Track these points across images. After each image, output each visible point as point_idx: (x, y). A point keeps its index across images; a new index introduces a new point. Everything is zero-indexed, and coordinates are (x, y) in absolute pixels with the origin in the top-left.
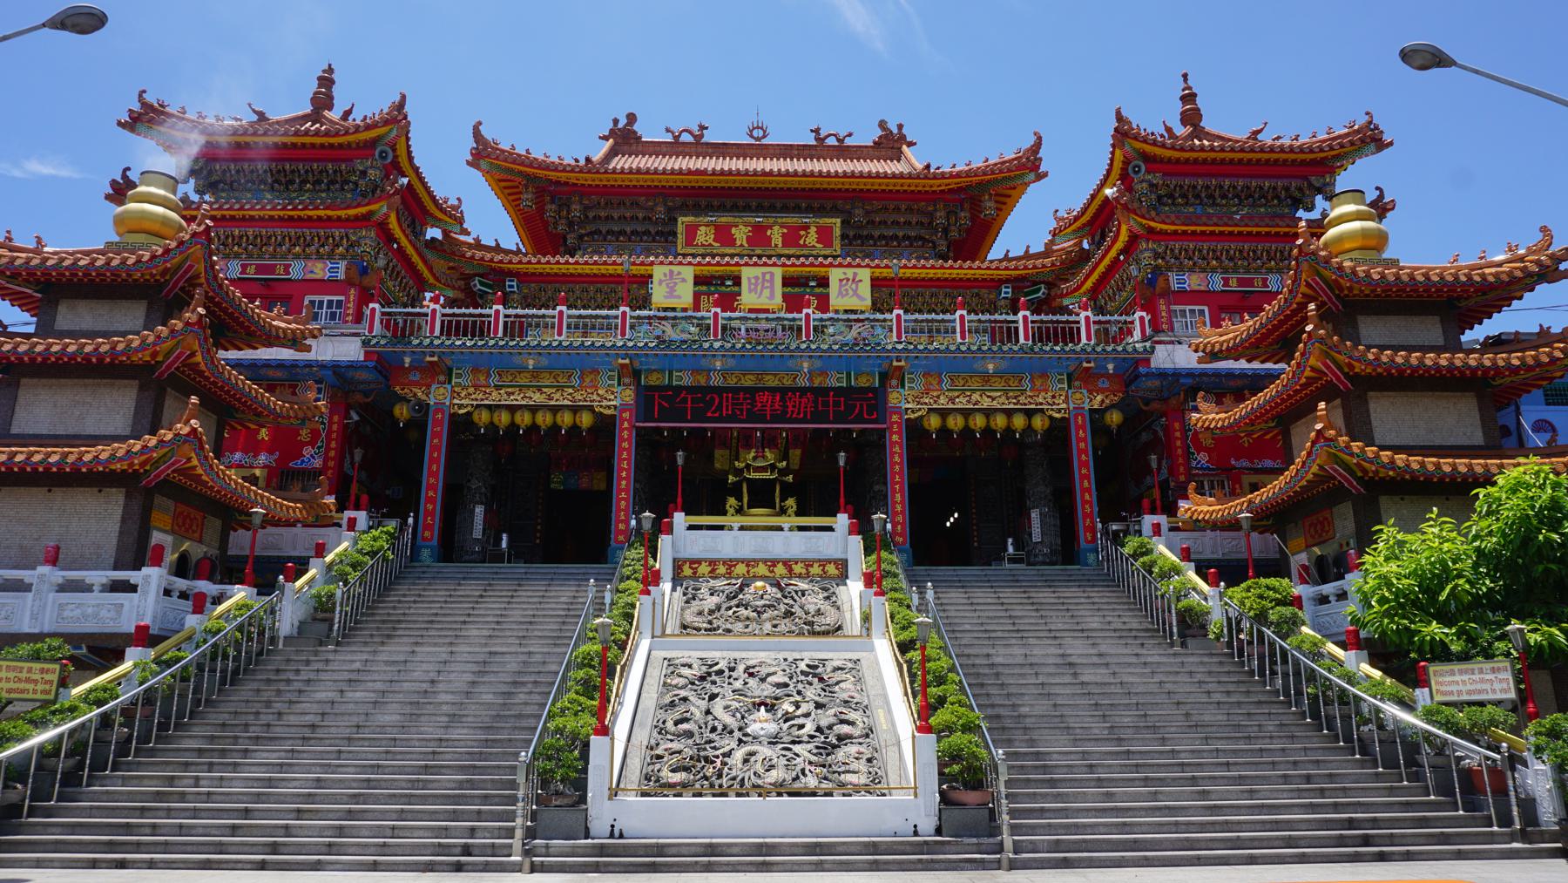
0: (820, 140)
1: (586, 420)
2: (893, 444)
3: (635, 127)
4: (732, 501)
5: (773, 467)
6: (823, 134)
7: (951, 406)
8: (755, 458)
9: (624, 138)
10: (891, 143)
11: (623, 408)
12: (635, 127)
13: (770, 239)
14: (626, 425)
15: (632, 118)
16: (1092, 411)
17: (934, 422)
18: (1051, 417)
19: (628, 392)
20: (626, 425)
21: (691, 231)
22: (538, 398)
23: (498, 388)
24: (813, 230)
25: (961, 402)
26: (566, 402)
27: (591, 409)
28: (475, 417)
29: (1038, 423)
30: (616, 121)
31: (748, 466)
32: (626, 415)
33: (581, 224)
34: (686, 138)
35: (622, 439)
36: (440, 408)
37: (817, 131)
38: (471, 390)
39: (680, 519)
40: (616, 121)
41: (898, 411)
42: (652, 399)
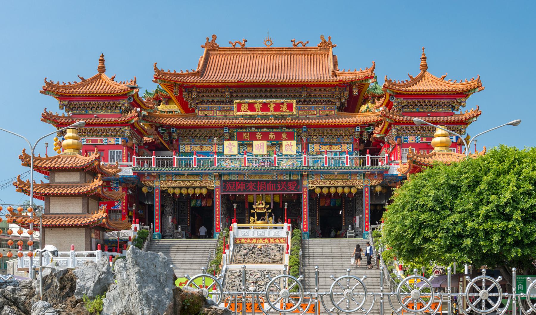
1: (204, 191)
2: (304, 198)
3: (216, 42)
4: (252, 218)
5: (264, 208)
7: (324, 185)
8: (259, 204)
9: (212, 48)
12: (216, 42)
13: (269, 108)
14: (217, 193)
15: (214, 37)
16: (371, 186)
17: (318, 191)
18: (358, 189)
19: (218, 182)
20: (217, 193)
21: (239, 106)
22: (188, 184)
23: (175, 181)
24: (285, 104)
25: (328, 184)
26: (198, 186)
27: (206, 187)
30: (208, 39)
31: (257, 208)
33: (197, 99)
34: (238, 46)
35: (217, 198)
38: (166, 182)
39: (235, 225)
40: (208, 39)
41: (306, 187)
42: (225, 184)
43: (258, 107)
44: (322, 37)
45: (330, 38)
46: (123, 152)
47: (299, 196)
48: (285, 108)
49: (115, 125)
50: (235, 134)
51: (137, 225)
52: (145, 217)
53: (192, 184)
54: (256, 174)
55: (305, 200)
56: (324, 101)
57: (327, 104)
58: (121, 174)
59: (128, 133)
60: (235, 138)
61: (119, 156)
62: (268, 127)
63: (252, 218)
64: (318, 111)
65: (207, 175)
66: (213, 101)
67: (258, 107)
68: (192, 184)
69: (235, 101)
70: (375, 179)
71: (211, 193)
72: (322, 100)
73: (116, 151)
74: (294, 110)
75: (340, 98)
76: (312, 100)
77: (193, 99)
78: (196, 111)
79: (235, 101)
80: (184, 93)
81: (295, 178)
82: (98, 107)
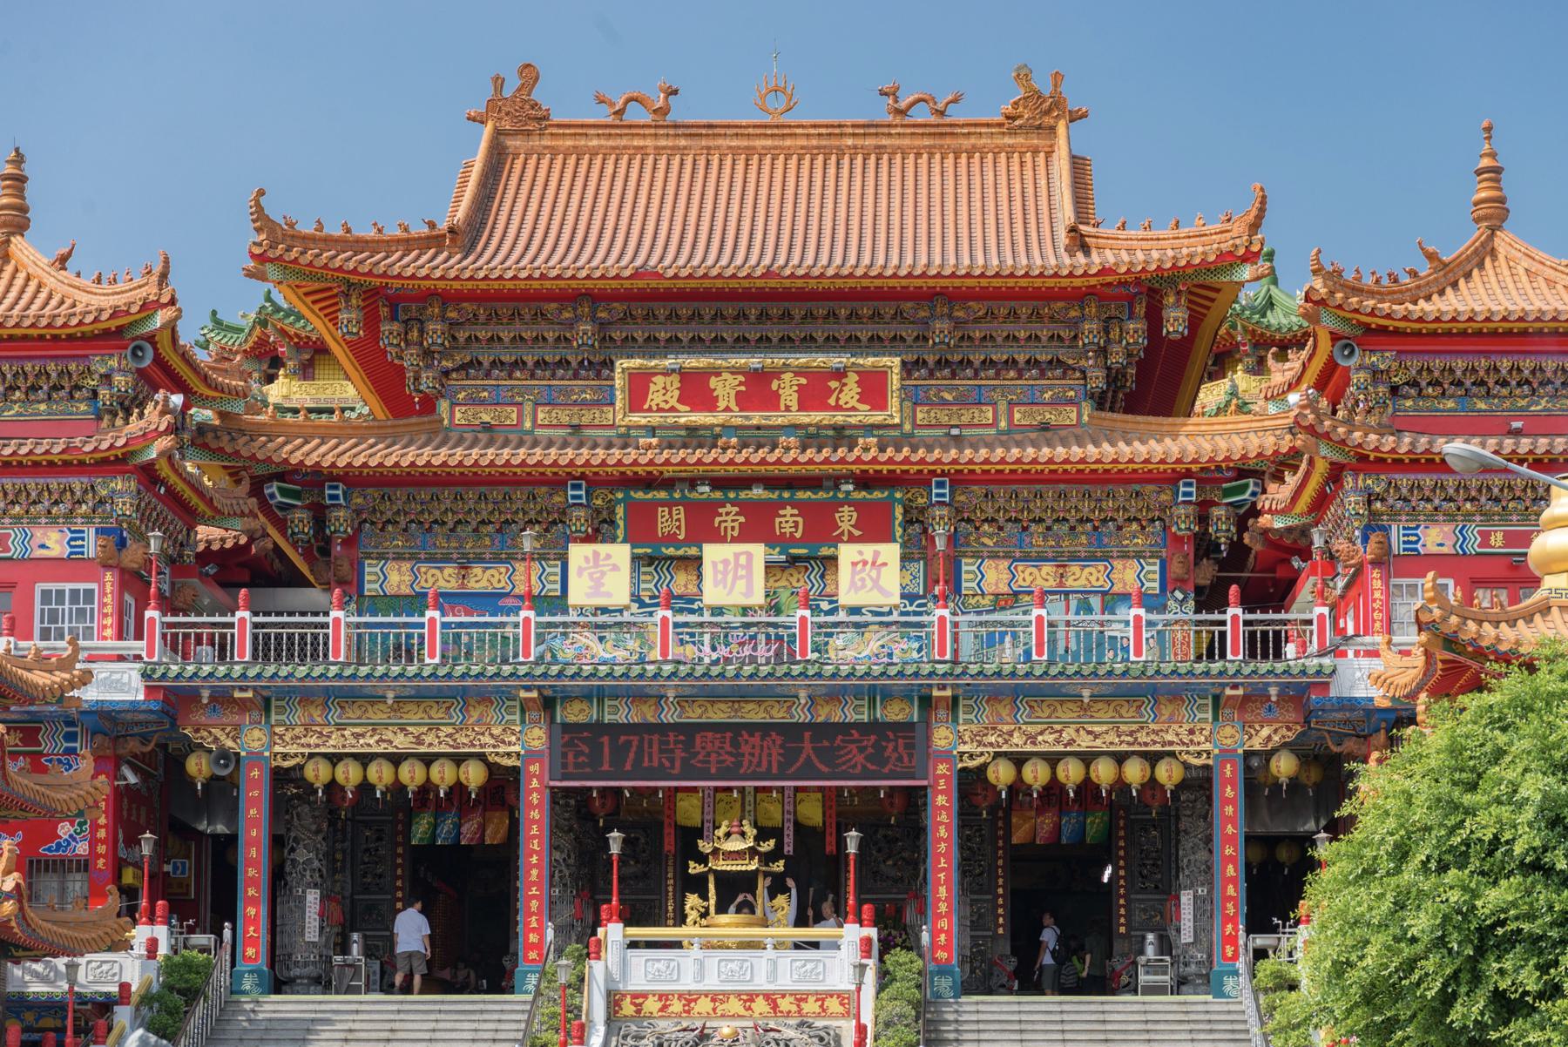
17: (1002, 774)
24: (852, 378)
41: (946, 756)
42: (576, 742)
50: (620, 511)
53: (420, 742)
55: (943, 817)
56: (1032, 363)
62: (770, 482)
65: (485, 698)
68: (420, 742)
72: (1021, 358)
74: (894, 402)
75: (1103, 352)
77: (427, 354)
78: (443, 406)
79: (622, 364)
80: (385, 327)
81: (895, 713)
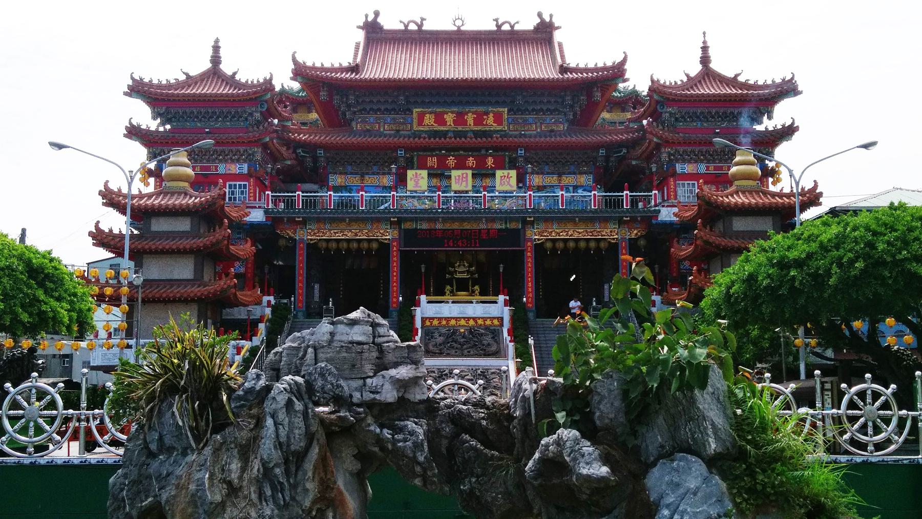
0: (499, 26)
1: (375, 245)
6: (500, 22)
9: (374, 34)
10: (544, 34)
11: (394, 240)
15: (377, 14)
17: (549, 245)
22: (350, 235)
24: (491, 115)
28: (320, 245)
29: (602, 245)
30: (367, 16)
32: (395, 244)
34: (413, 27)
36: (302, 240)
37: (496, 20)
40: (367, 16)
41: (531, 240)
42: (409, 237)
43: (449, 118)
44: (540, 15)
45: (551, 16)
46: (250, 185)
47: (522, 253)
48: (490, 120)
49: (239, 144)
50: (415, 159)
51: (271, 298)
52: (282, 285)
53: (356, 235)
54: (453, 220)
55: (530, 260)
56: (548, 110)
57: (551, 114)
58: (247, 219)
59: (258, 157)
60: (415, 166)
61: (242, 193)
62: (465, 150)
63: (448, 287)
64: (538, 124)
65: (378, 220)
66: (379, 110)
67: (449, 118)
68: (356, 235)
69: (415, 110)
70: (637, 228)
71: (384, 247)
72: (545, 108)
73: (238, 183)
74: (505, 123)
75: (572, 106)
76: (530, 108)
77: (349, 106)
78: (354, 124)
79: (415, 110)
80: (335, 97)
81: (512, 226)
82: (211, 117)
